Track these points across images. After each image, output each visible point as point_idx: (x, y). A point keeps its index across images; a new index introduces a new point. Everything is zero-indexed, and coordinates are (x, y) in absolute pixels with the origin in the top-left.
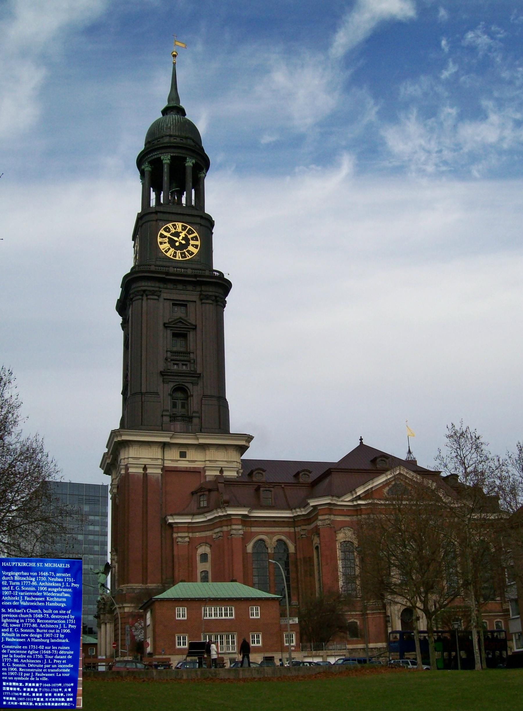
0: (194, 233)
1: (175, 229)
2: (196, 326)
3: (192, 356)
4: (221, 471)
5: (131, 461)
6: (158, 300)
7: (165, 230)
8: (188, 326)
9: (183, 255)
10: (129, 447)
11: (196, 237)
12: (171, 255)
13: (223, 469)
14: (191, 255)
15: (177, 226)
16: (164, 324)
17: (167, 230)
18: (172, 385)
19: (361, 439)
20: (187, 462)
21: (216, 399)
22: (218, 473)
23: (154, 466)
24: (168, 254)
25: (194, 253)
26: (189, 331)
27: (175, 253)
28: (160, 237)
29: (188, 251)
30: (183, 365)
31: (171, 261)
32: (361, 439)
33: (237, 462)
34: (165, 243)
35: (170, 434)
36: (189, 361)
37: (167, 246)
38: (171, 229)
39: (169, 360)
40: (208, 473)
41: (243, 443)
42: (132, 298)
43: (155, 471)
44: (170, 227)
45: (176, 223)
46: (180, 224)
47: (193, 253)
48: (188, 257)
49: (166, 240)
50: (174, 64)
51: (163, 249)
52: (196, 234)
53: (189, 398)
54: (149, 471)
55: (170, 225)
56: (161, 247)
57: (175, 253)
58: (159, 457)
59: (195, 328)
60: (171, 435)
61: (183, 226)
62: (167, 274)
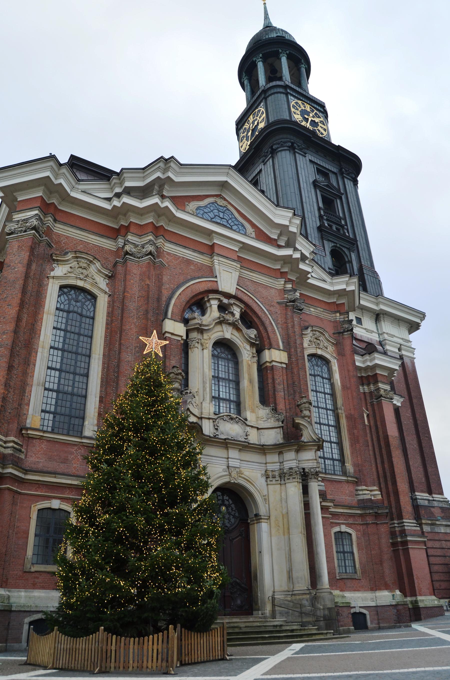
1: (305, 107)
3: (343, 222)
6: (305, 157)
20: (364, 331)
26: (336, 198)
29: (319, 131)
34: (298, 114)
39: (325, 217)
41: (418, 321)
42: (278, 148)
45: (305, 104)
46: (309, 106)
47: (322, 134)
53: (348, 265)
55: (300, 102)
61: (310, 108)
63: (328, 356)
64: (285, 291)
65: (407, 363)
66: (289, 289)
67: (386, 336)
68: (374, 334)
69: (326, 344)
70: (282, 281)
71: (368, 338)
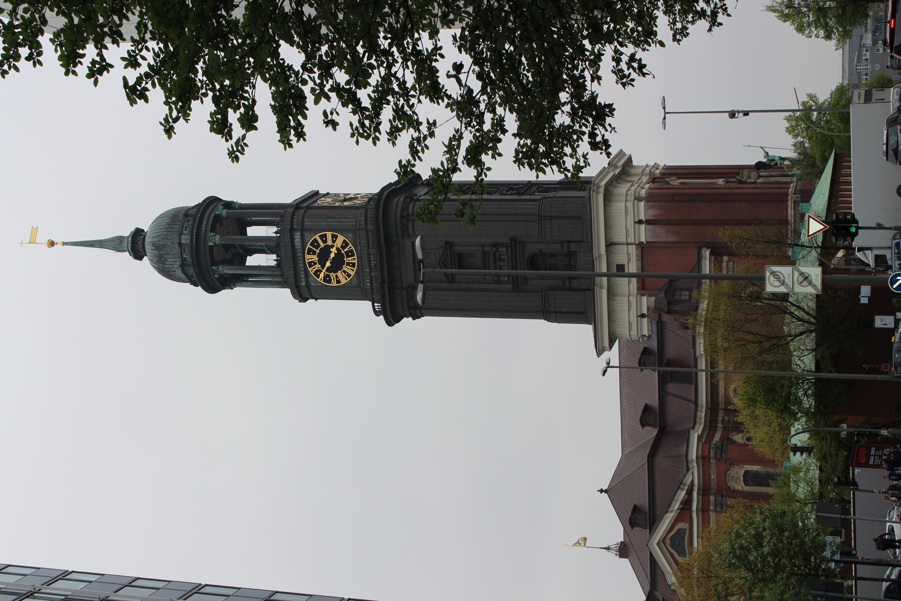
0: (315, 238)
1: (315, 264)
2: (447, 243)
3: (487, 249)
4: (640, 222)
5: (634, 332)
7: (318, 276)
8: (447, 254)
9: (350, 254)
10: (616, 334)
12: (353, 270)
13: (636, 221)
15: (311, 260)
16: (449, 282)
17: (317, 273)
21: (543, 221)
23: (639, 305)
24: (352, 273)
25: (344, 240)
26: (454, 251)
27: (348, 264)
28: (330, 284)
29: (343, 247)
30: (500, 260)
31: (361, 267)
33: (626, 201)
34: (337, 276)
35: (597, 289)
36: (495, 253)
38: (316, 269)
40: (643, 240)
44: (314, 270)
46: (307, 257)
47: (344, 241)
48: (351, 247)
49: (332, 275)
50: (64, 244)
51: (346, 279)
52: (317, 237)
54: (645, 311)
55: (311, 270)
56: (343, 282)
57: (348, 264)
58: (627, 299)
59: (449, 244)
60: (598, 289)
61: (308, 253)
62: (383, 282)
63: (743, 472)
64: (715, 511)
65: (653, 216)
66: (713, 509)
67: (631, 240)
68: (630, 252)
69: (734, 472)
70: (711, 513)
71: (637, 260)
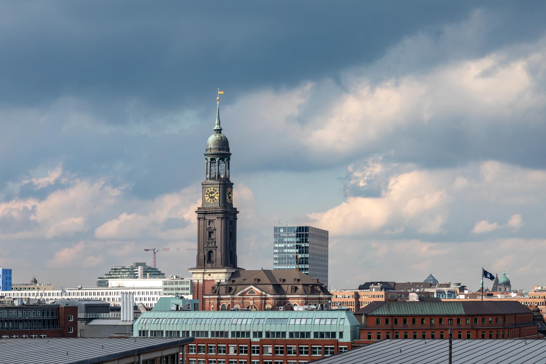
3: (214, 239)
11: (217, 193)
14: (216, 200)
18: (208, 251)
19: (262, 268)
22: (219, 281)
24: (208, 201)
27: (211, 200)
29: (215, 199)
32: (262, 268)
37: (208, 197)
43: (201, 282)
46: (212, 188)
47: (216, 199)
49: (208, 195)
55: (209, 189)
56: (206, 198)
57: (211, 200)
61: (213, 189)
